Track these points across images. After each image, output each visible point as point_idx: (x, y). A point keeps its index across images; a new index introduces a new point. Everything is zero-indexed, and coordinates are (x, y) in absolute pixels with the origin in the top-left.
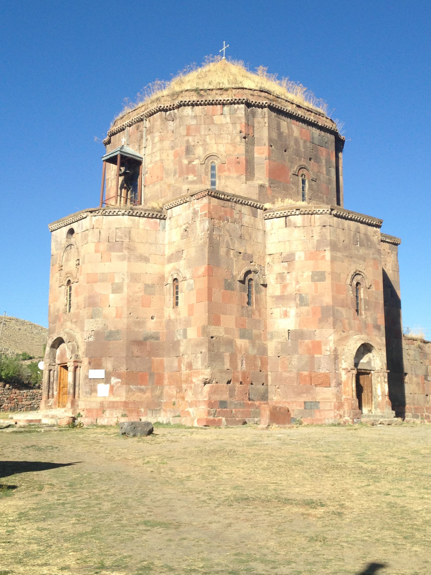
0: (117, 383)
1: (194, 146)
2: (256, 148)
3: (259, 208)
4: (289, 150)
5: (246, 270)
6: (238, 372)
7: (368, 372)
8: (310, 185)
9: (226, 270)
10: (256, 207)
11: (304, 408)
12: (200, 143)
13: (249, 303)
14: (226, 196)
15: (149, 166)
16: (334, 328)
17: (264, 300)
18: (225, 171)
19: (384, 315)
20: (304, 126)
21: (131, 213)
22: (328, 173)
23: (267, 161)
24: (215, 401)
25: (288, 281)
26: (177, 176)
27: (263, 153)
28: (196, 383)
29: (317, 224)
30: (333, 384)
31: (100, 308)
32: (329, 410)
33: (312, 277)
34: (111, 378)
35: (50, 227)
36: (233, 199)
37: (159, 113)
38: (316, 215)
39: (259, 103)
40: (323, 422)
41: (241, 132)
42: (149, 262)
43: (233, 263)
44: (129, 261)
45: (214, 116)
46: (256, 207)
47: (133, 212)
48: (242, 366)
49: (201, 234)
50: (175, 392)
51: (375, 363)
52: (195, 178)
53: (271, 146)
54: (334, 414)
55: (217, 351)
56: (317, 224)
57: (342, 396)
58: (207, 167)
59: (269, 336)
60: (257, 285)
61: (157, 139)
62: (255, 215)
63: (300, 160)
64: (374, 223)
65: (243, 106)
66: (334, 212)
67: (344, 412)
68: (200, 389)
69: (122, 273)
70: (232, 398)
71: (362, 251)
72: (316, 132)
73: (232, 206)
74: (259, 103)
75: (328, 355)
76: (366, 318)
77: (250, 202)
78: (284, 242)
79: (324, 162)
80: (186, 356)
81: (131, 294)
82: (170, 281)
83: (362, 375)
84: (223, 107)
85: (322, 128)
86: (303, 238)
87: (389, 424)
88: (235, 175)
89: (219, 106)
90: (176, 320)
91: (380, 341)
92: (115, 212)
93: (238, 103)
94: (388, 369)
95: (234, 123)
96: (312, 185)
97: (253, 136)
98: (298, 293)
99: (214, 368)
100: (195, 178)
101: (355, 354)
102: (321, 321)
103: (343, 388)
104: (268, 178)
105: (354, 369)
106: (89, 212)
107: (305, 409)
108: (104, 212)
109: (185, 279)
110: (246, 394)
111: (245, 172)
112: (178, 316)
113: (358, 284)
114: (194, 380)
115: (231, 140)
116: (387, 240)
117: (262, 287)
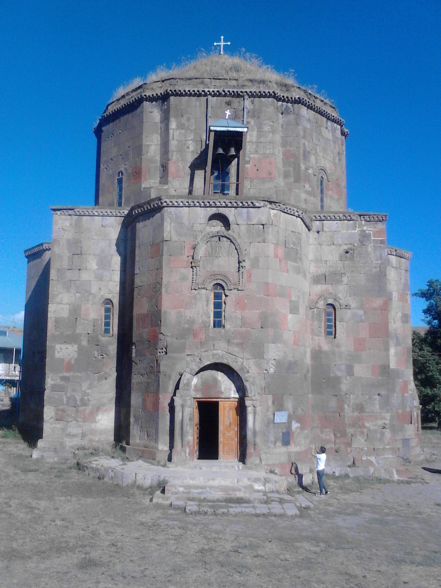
0: (297, 428)
15: (252, 156)
26: (292, 180)
28: (372, 428)
29: (403, 268)
31: (280, 331)
34: (292, 422)
35: (168, 201)
37: (270, 99)
49: (376, 262)
50: (333, 436)
52: (310, 189)
61: (266, 128)
68: (379, 436)
80: (352, 396)
82: (321, 304)
90: (333, 353)
92: (293, 210)
93: (337, 123)
100: (310, 189)
106: (268, 201)
108: (284, 207)
109: (347, 307)
112: (336, 349)
114: (367, 424)
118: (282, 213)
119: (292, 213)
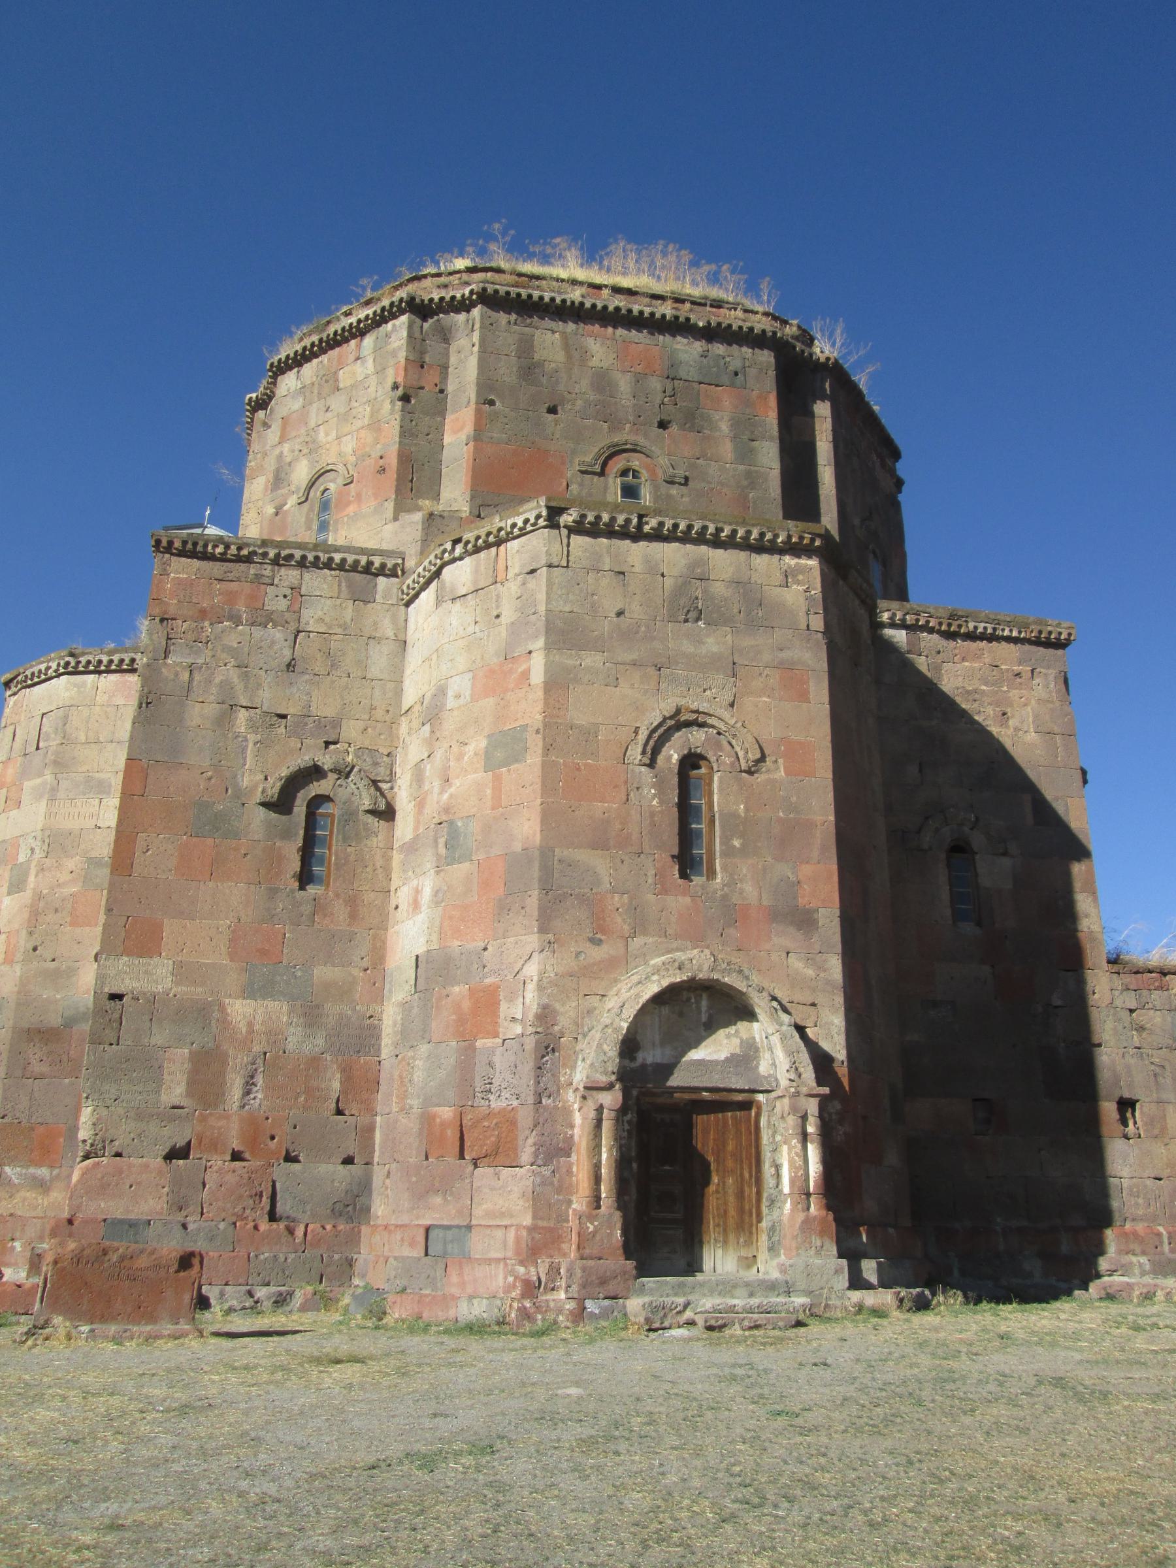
1: (290, 464)
2: (449, 419)
3: (382, 571)
4: (568, 407)
5: (293, 768)
6: (228, 1117)
7: (740, 1097)
8: (656, 498)
9: (210, 773)
10: (367, 570)
11: (422, 1253)
12: (305, 451)
13: (305, 878)
14: (233, 547)
16: (542, 930)
17: (379, 862)
18: (349, 503)
19: (834, 868)
20: (639, 337)
21: (73, 664)
22: (745, 454)
23: (472, 444)
24: (86, 1222)
25: (426, 788)
27: (461, 429)
30: (526, 1156)
32: (489, 1261)
33: (488, 754)
36: (265, 555)
38: (509, 543)
39: (453, 298)
40: (452, 1313)
41: (395, 387)
42: (109, 793)
43: (244, 750)
44: (52, 799)
45: (341, 372)
46: (367, 570)
47: (78, 663)
48: (248, 1093)
51: (777, 1062)
53: (491, 403)
54: (505, 1278)
55: (129, 1043)
56: (511, 575)
57: (570, 1202)
58: (311, 509)
59: (387, 987)
60: (350, 815)
62: (363, 598)
63: (616, 427)
64: (779, 540)
65: (404, 318)
66: (567, 519)
67: (554, 1271)
69: (33, 834)
70: (184, 1213)
71: (715, 642)
72: (688, 349)
73: (258, 576)
74: (453, 298)
75: (518, 1036)
76: (731, 883)
77: (337, 557)
78: (429, 659)
79: (724, 427)
81: (45, 892)
83: (708, 1112)
84: (361, 340)
85: (711, 334)
86: (471, 629)
87: (710, 1328)
88: (369, 505)
89: (353, 343)
91: (810, 972)
93: (394, 316)
94: (820, 1083)
95: (380, 371)
96: (669, 497)
97: (442, 391)
98: (444, 818)
99: (109, 1102)
101: (625, 1025)
102: (503, 909)
103: (574, 1169)
104: (468, 493)
105: (610, 1087)
107: (426, 1254)
110: (261, 1196)
111: (394, 489)
113: (691, 761)
115: (372, 416)
116: (1006, 633)
117: (370, 819)
118: (28, 690)
119: (43, 677)
